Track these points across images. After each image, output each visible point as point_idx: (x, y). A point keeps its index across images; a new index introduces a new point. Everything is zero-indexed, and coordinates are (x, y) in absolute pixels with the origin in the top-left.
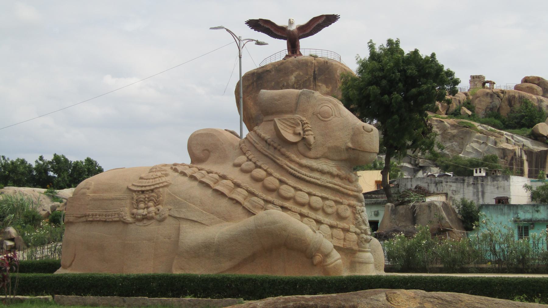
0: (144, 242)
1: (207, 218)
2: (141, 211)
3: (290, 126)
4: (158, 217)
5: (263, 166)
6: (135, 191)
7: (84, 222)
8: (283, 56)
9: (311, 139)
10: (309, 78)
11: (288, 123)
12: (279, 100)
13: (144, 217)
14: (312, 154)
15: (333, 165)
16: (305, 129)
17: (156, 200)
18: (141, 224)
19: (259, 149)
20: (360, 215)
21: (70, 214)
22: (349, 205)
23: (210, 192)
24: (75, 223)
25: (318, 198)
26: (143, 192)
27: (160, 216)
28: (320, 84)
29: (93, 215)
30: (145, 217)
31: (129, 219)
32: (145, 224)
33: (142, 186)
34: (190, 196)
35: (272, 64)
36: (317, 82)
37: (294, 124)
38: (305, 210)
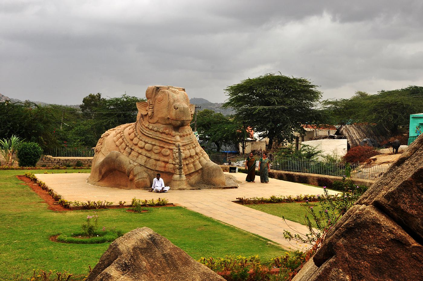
11: (143, 105)
22: (169, 149)
37: (146, 105)
38: (140, 151)
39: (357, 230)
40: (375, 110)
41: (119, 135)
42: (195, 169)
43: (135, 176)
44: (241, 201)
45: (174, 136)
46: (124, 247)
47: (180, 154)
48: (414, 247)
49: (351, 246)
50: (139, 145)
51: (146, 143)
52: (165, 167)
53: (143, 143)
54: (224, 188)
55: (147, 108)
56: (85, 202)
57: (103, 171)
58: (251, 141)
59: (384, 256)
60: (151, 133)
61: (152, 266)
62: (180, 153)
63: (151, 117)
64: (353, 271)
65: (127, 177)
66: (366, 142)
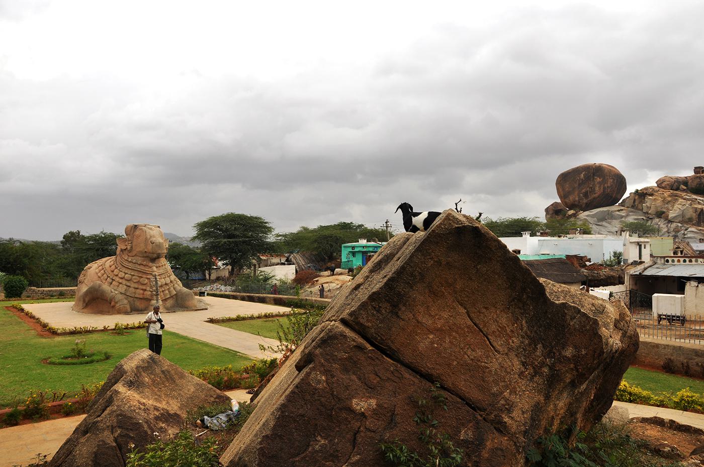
10: (590, 175)
22: (147, 278)
28: (596, 177)
38: (120, 281)
39: (329, 341)
40: (315, 241)
41: (101, 268)
42: (170, 294)
43: (116, 303)
44: (212, 321)
45: (151, 267)
46: (129, 367)
47: (156, 283)
48: (370, 350)
49: (325, 354)
50: (119, 275)
51: (126, 274)
52: (143, 294)
53: (124, 274)
54: (196, 310)
55: (127, 243)
56: (72, 328)
57: (87, 300)
58: (216, 268)
59: (350, 358)
61: (153, 381)
62: (156, 281)
63: (130, 251)
64: (328, 373)
66: (309, 267)
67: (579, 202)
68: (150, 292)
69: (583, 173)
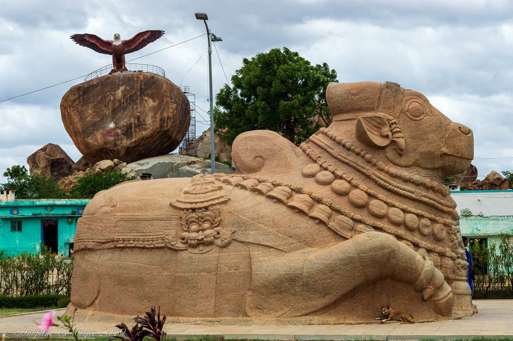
0: (203, 274)
1: (284, 243)
2: (194, 235)
3: (378, 127)
4: (218, 242)
5: (344, 176)
6: (182, 209)
7: (112, 248)
8: (109, 71)
9: (401, 142)
12: (356, 95)
13: (199, 242)
14: (403, 161)
15: (425, 175)
16: (395, 130)
17: (214, 221)
18: (196, 251)
19: (335, 155)
20: (456, 236)
21: (88, 239)
22: (445, 224)
23: (284, 208)
24: (97, 250)
25: (414, 215)
26: (194, 210)
27: (222, 241)
28: (146, 98)
29: (124, 240)
30: (201, 242)
31: (180, 245)
32: (202, 250)
33: (192, 203)
34: (258, 214)
35: (98, 79)
36: (143, 96)
37: (379, 124)
55: (386, 130)
60: (413, 190)
65: (412, 293)
67: (116, 145)
68: (451, 262)
69: (122, 88)
